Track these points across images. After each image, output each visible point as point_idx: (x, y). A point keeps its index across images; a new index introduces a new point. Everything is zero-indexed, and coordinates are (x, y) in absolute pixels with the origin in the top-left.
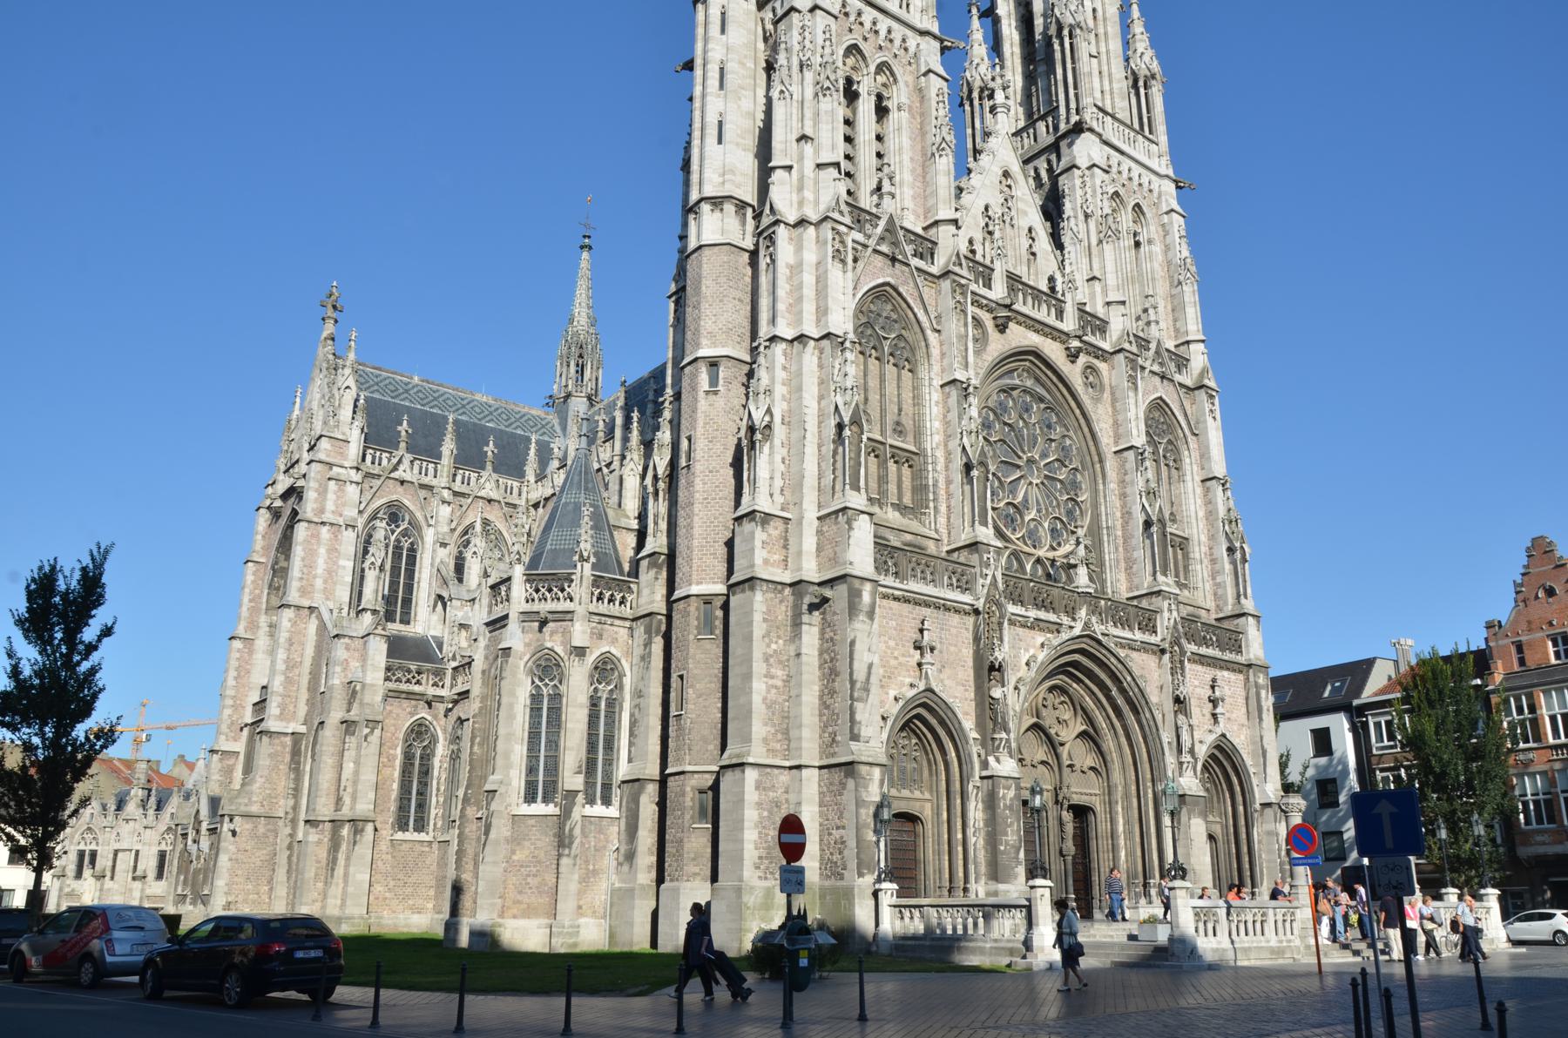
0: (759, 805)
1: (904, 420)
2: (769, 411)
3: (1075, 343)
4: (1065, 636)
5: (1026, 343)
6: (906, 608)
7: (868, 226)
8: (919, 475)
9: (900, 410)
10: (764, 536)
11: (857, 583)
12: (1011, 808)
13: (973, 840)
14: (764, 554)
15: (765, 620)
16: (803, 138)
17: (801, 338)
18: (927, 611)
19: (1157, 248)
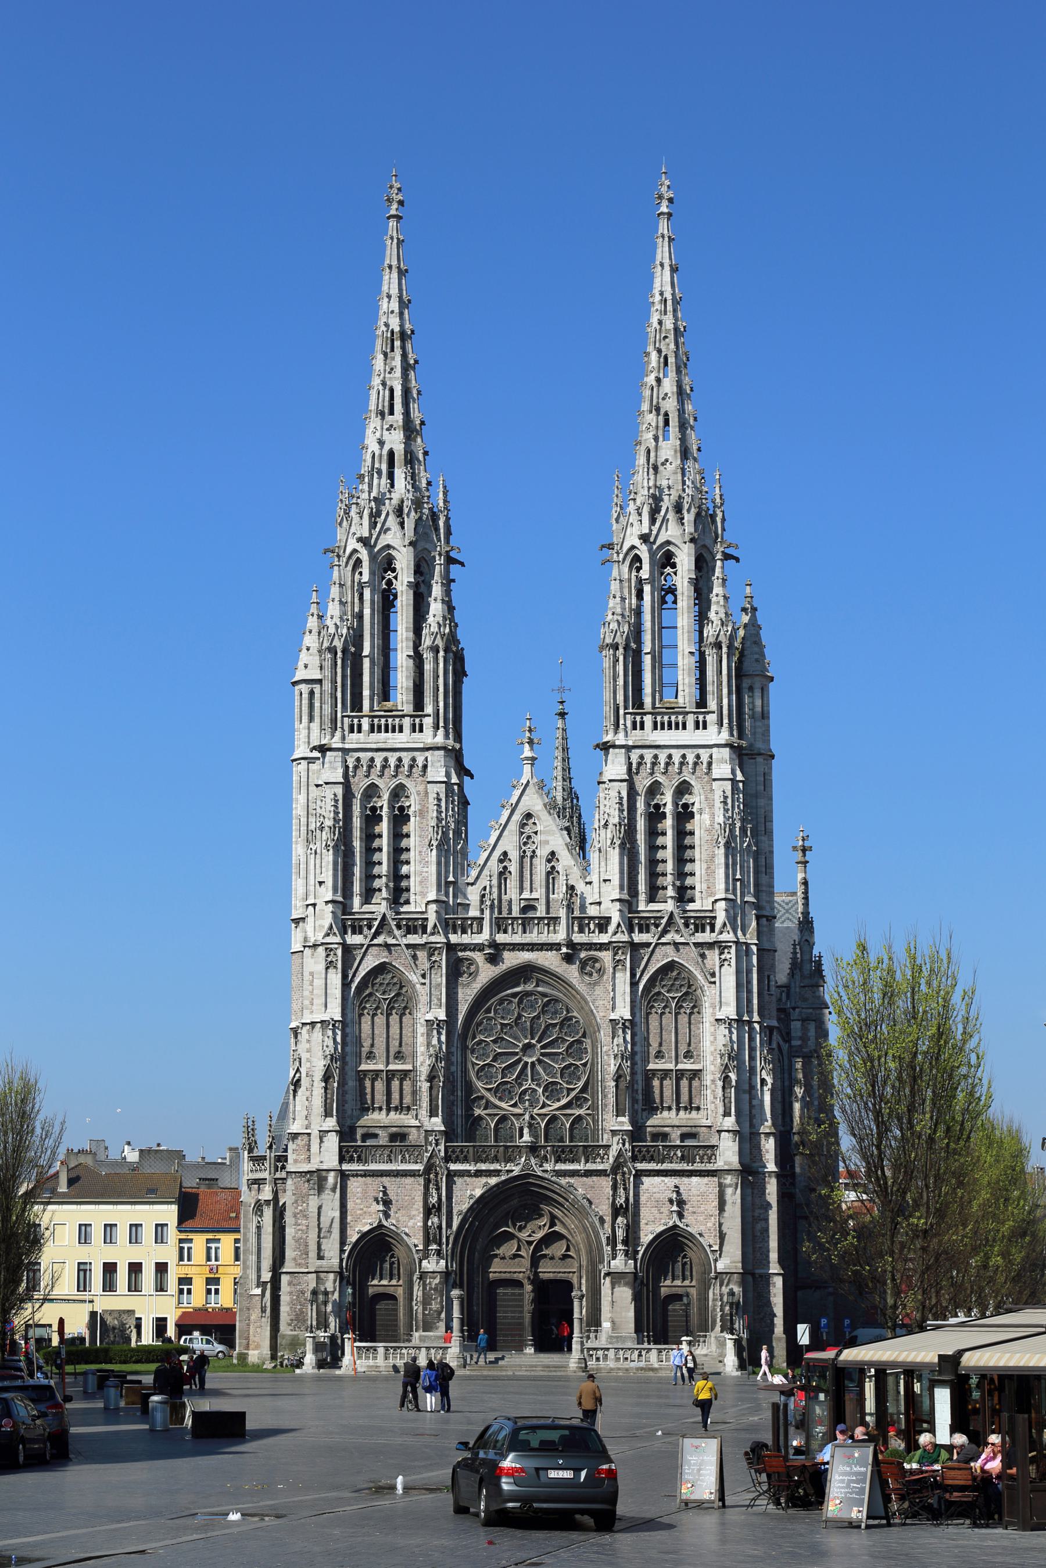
0: (291, 1293)
1: (404, 1049)
2: (298, 1070)
3: (564, 950)
4: (503, 1178)
5: (519, 961)
6: (369, 1180)
7: (365, 929)
8: (414, 1082)
9: (400, 1045)
10: (294, 1146)
11: (324, 1174)
12: (435, 1289)
13: (415, 1308)
14: (294, 1156)
15: (294, 1194)
16: (321, 883)
17: (313, 1024)
18: (385, 1180)
19: (706, 817)
